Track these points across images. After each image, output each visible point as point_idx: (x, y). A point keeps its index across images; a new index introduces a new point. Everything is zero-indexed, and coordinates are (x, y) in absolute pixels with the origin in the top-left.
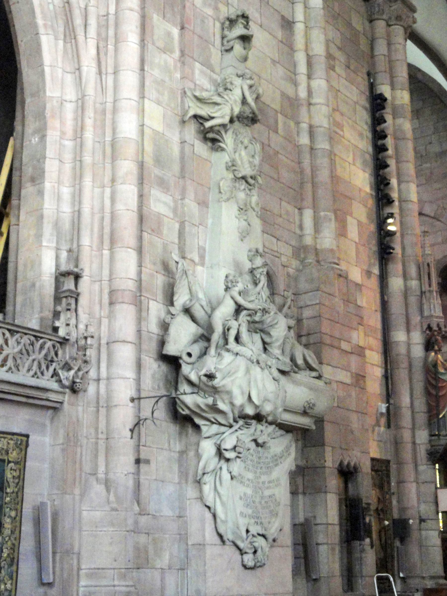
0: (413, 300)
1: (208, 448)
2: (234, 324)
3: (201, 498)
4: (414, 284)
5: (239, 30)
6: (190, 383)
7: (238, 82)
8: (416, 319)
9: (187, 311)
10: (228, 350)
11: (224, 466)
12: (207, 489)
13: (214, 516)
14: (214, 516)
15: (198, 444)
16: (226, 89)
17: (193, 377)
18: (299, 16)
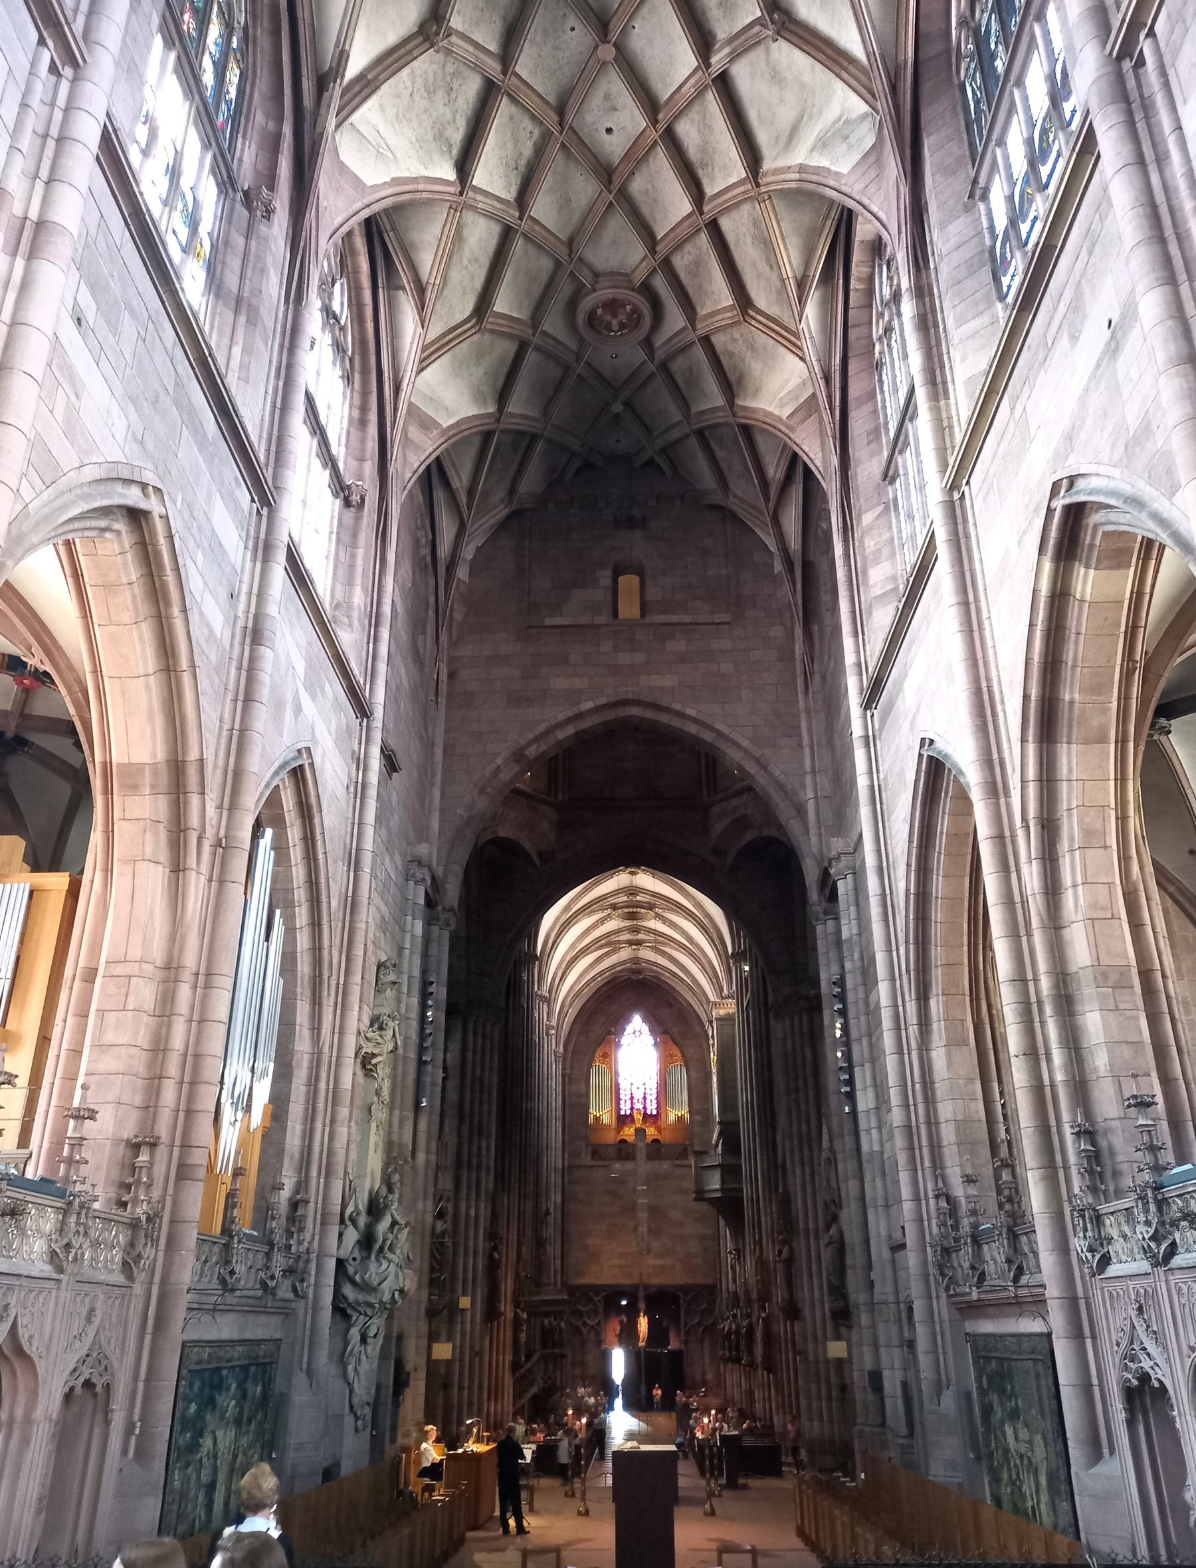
0: (431, 1173)
1: (355, 1334)
2: (391, 1236)
3: (345, 1376)
4: (433, 1158)
5: (392, 977)
6: (353, 1282)
7: (391, 1024)
8: (431, 1189)
9: (353, 1221)
10: (385, 1258)
11: (362, 1348)
12: (350, 1368)
13: (351, 1391)
14: (351, 1391)
15: (347, 1331)
16: (381, 1028)
17: (358, 1278)
18: (407, 945)
